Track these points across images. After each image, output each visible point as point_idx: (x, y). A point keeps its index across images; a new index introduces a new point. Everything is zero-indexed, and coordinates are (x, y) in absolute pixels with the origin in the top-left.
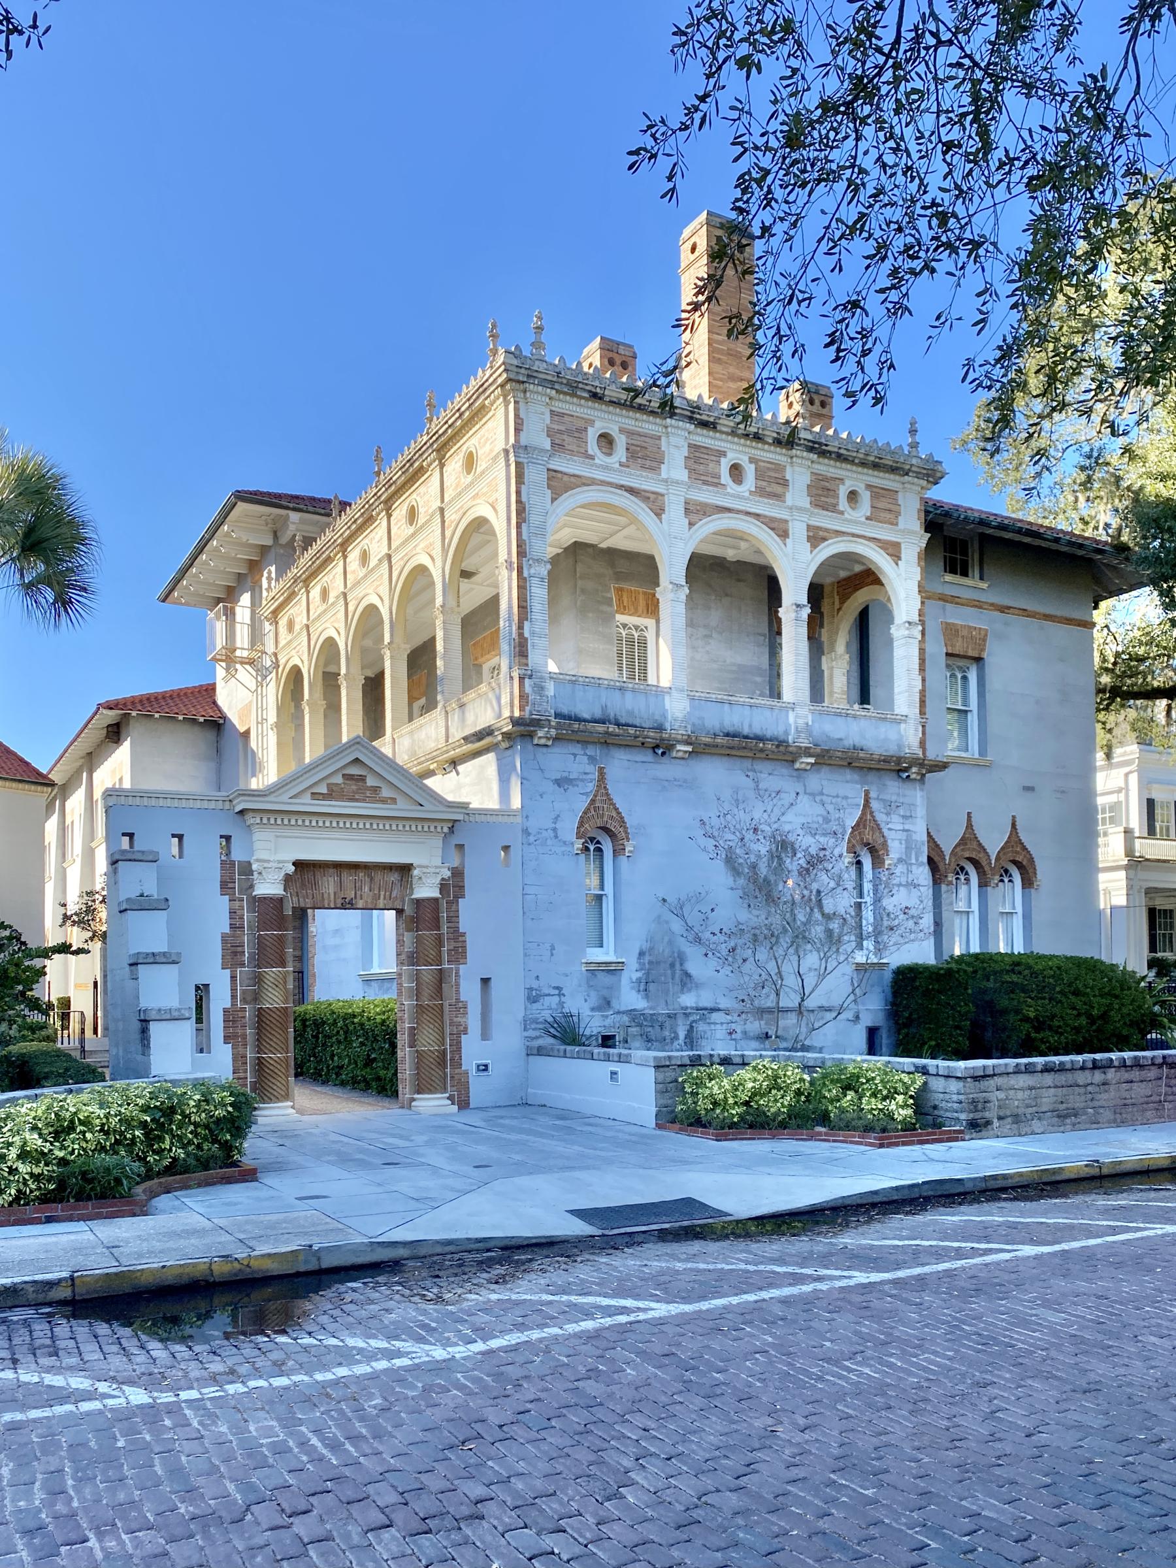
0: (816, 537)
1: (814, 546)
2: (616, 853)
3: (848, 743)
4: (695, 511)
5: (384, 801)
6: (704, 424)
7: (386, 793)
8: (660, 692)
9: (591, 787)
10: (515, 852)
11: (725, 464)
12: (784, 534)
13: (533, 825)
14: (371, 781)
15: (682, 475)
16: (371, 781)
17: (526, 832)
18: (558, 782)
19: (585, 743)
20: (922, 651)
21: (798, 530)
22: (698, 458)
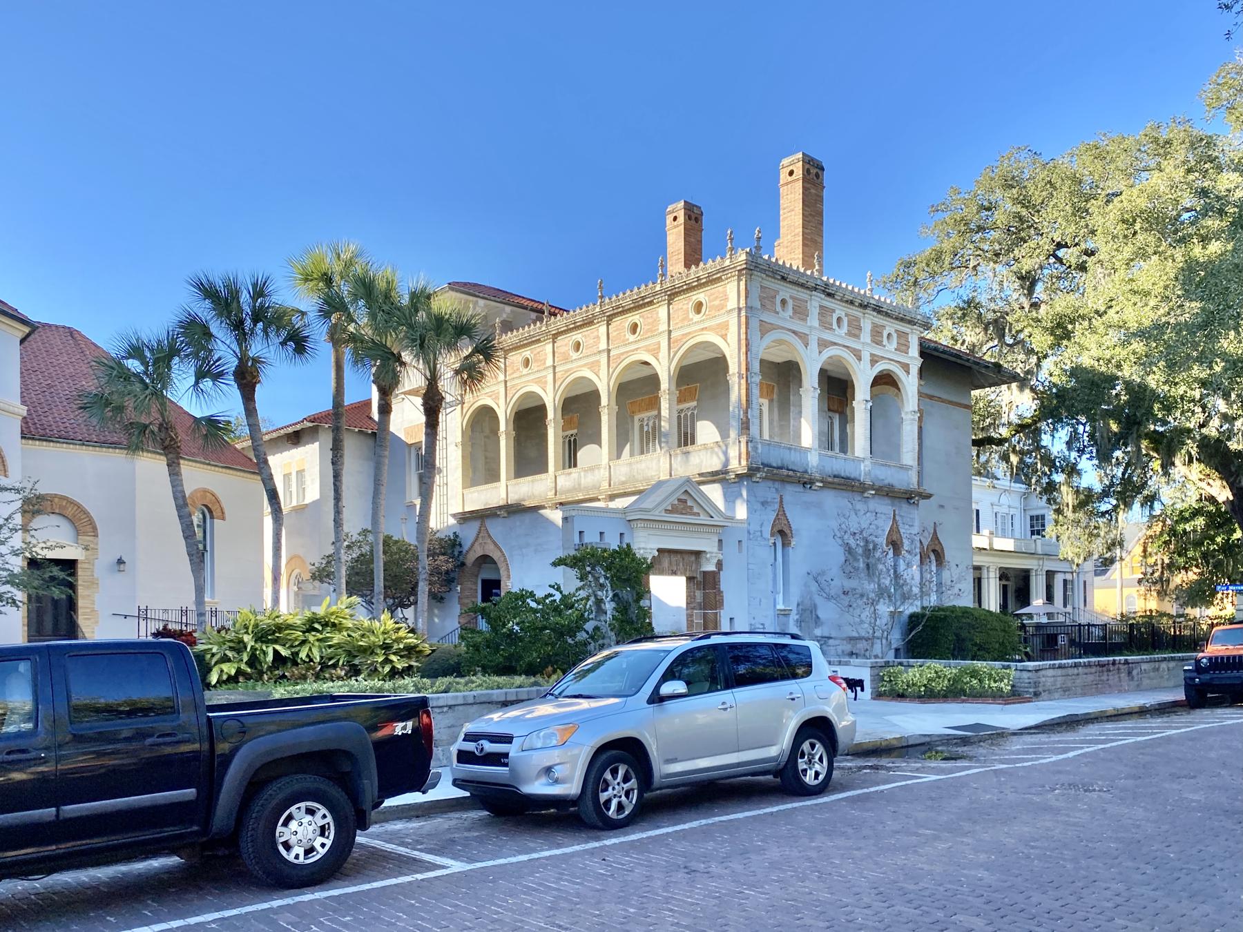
0: (874, 360)
1: (872, 366)
2: (783, 545)
3: (886, 482)
4: (823, 344)
5: (695, 514)
6: (829, 295)
7: (696, 510)
8: (807, 450)
9: (777, 506)
10: (744, 544)
11: (835, 317)
12: (860, 359)
13: (752, 529)
14: (690, 503)
15: (816, 323)
16: (690, 503)
17: (749, 532)
18: (764, 504)
19: (774, 480)
20: (920, 428)
21: (866, 356)
22: (824, 312)
